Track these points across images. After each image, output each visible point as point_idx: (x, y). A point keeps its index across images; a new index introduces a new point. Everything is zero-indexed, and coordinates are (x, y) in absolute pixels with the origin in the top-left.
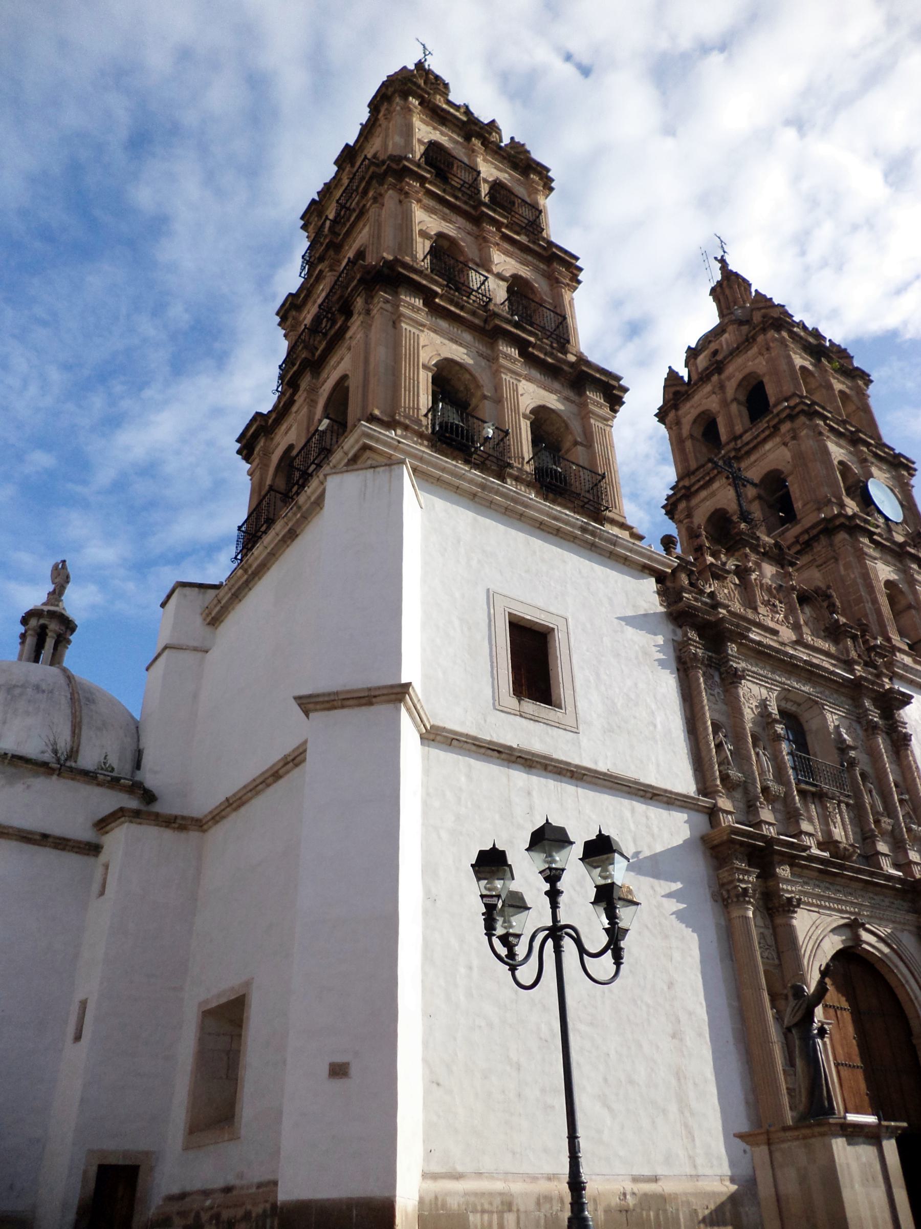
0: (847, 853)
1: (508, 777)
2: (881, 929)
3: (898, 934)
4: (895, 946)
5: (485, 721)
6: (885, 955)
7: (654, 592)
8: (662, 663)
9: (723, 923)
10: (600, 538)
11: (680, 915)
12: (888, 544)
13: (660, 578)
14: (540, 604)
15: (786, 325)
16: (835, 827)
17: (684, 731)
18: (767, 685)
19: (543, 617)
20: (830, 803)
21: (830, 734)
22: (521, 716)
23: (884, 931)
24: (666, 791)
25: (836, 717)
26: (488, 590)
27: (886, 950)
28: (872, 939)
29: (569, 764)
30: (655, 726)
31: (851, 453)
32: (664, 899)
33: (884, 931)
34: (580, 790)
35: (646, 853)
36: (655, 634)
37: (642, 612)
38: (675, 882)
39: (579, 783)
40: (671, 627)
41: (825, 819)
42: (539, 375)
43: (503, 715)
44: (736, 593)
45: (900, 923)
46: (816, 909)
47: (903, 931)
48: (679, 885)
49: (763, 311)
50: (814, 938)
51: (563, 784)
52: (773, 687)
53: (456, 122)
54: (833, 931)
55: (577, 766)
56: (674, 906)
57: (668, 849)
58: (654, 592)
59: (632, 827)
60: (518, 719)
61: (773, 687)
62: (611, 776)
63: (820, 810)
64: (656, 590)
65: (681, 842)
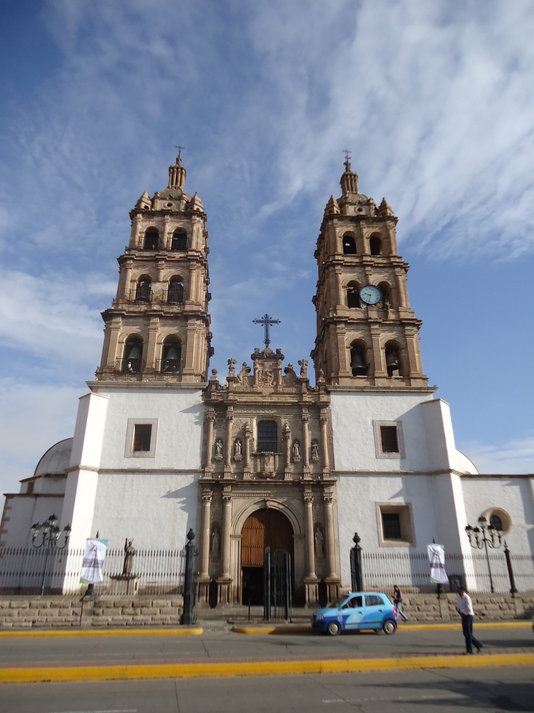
0: (267, 475)
1: (126, 477)
2: (281, 500)
3: (291, 501)
4: (286, 505)
5: (121, 462)
6: (281, 509)
7: (200, 396)
8: (196, 423)
9: (201, 508)
10: (174, 386)
11: (182, 508)
12: (359, 321)
13: (203, 390)
14: (148, 417)
15: (335, 216)
16: (267, 466)
17: (200, 446)
18: (250, 416)
19: (148, 421)
20: (267, 457)
21: (281, 427)
22: (134, 457)
23: (281, 501)
24: (183, 470)
25: (288, 419)
26: (128, 419)
27: (281, 507)
28: (275, 504)
29: (145, 470)
30: (188, 447)
31: (360, 273)
32: (178, 504)
33: (281, 501)
34: (152, 476)
35: (174, 490)
36: (196, 413)
37: (192, 406)
38: (183, 497)
39: (152, 473)
40: (205, 407)
41: (263, 463)
42: (170, 321)
43: (127, 458)
44: (247, 381)
45: (292, 497)
46: (248, 498)
47: (294, 499)
48: (185, 499)
49: (329, 210)
50: (243, 507)
51: (146, 475)
52: (253, 416)
53: (158, 213)
54: (255, 504)
55: (148, 470)
56: (181, 505)
57: (183, 488)
58: (200, 396)
59: (170, 483)
60: (133, 458)
61: (253, 416)
62: (161, 470)
63: (262, 460)
64: (201, 394)
65: (189, 484)
